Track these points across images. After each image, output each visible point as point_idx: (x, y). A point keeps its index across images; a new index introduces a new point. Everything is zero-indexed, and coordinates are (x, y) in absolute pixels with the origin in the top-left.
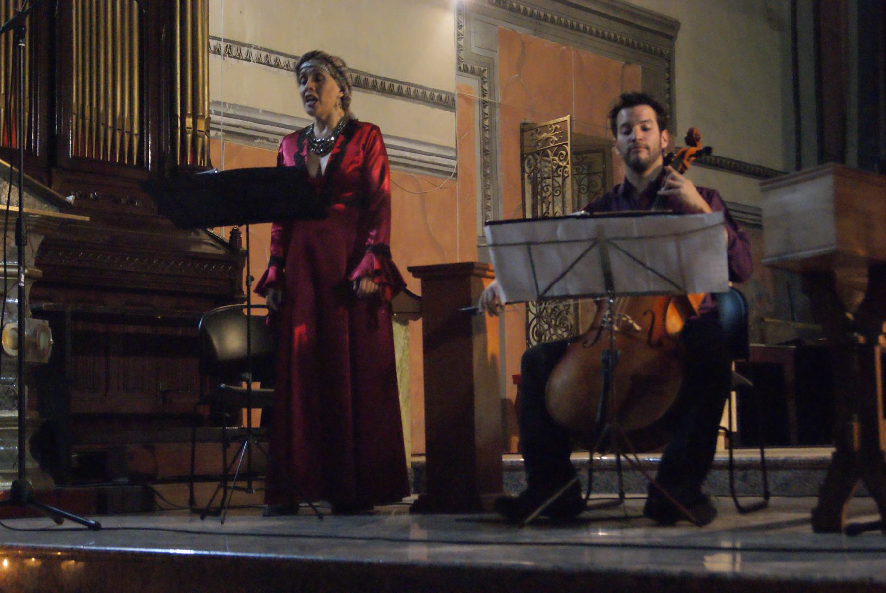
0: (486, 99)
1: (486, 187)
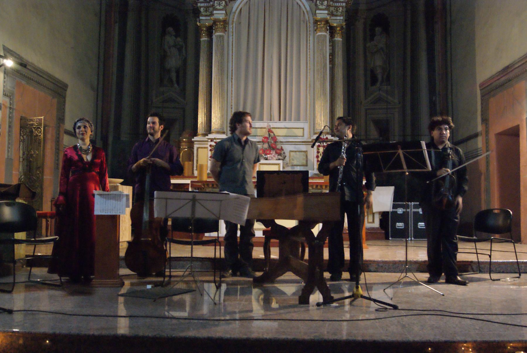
0: (11, 106)
1: (9, 140)
